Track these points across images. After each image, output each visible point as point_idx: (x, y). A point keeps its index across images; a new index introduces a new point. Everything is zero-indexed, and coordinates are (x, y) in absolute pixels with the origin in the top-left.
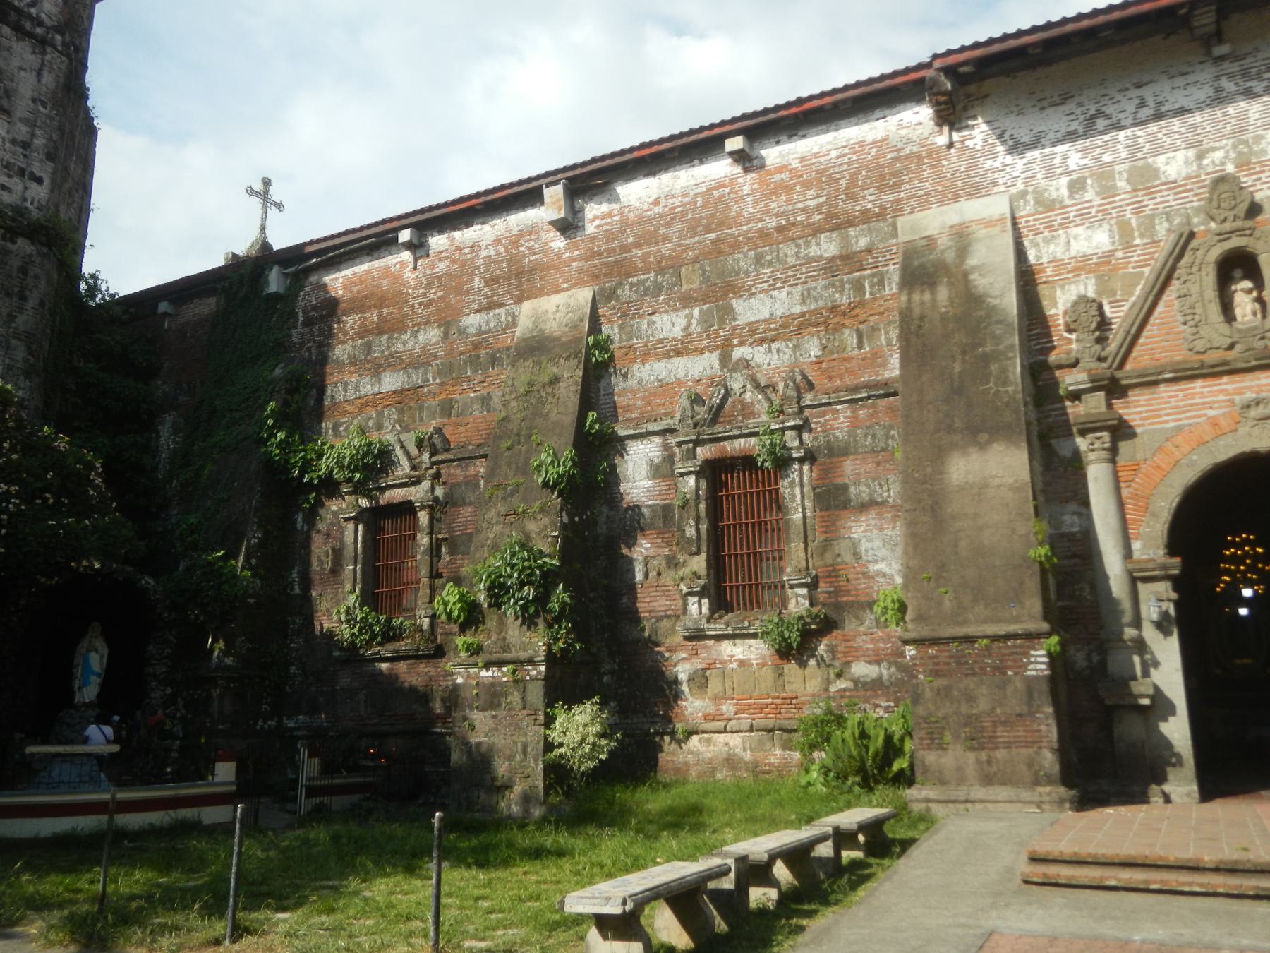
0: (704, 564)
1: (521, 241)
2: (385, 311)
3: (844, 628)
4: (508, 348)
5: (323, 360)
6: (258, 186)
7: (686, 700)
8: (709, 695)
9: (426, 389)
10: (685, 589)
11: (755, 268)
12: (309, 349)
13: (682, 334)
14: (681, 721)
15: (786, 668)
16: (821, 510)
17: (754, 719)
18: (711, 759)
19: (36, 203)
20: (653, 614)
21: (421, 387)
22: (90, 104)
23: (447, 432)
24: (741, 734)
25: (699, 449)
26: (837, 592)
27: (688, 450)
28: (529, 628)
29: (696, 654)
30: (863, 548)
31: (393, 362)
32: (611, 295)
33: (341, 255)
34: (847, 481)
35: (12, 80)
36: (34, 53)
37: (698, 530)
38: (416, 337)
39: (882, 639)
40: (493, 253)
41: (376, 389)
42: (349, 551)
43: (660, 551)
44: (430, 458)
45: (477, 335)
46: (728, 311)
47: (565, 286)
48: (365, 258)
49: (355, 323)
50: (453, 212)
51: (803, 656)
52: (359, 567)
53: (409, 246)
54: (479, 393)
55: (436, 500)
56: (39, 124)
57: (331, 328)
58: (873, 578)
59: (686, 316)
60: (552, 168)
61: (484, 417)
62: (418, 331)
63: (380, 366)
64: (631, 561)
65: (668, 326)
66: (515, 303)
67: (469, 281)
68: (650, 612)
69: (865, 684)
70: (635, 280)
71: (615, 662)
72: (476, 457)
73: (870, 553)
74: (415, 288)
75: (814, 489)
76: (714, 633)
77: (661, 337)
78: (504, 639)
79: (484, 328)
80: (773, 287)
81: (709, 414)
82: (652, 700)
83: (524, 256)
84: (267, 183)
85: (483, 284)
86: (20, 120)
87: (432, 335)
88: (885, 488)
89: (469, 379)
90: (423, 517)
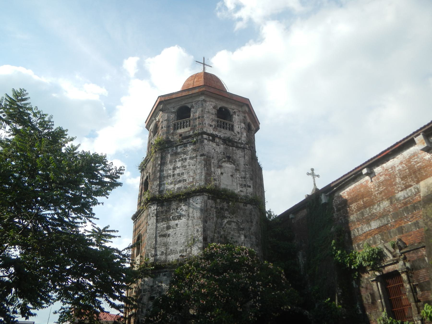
1: (412, 160)
2: (365, 199)
4: (419, 201)
5: (347, 222)
6: (310, 172)
9: (389, 225)
12: (341, 219)
19: (250, 193)
21: (387, 224)
22: (258, 161)
23: (404, 240)
31: (373, 217)
33: (344, 184)
35: (238, 161)
36: (242, 152)
38: (379, 206)
40: (401, 168)
41: (370, 229)
42: (377, 294)
44: (400, 251)
45: (403, 200)
48: (352, 183)
49: (355, 206)
50: (380, 158)
52: (383, 300)
53: (367, 174)
54: (412, 222)
55: (407, 268)
56: (247, 171)
57: (347, 210)
60: (415, 130)
61: (418, 231)
62: (380, 204)
63: (369, 219)
67: (394, 181)
74: (374, 188)
79: (406, 196)
83: (414, 165)
84: (312, 170)
85: (400, 180)
86: (242, 171)
87: (386, 204)
89: (406, 217)
90: (404, 276)
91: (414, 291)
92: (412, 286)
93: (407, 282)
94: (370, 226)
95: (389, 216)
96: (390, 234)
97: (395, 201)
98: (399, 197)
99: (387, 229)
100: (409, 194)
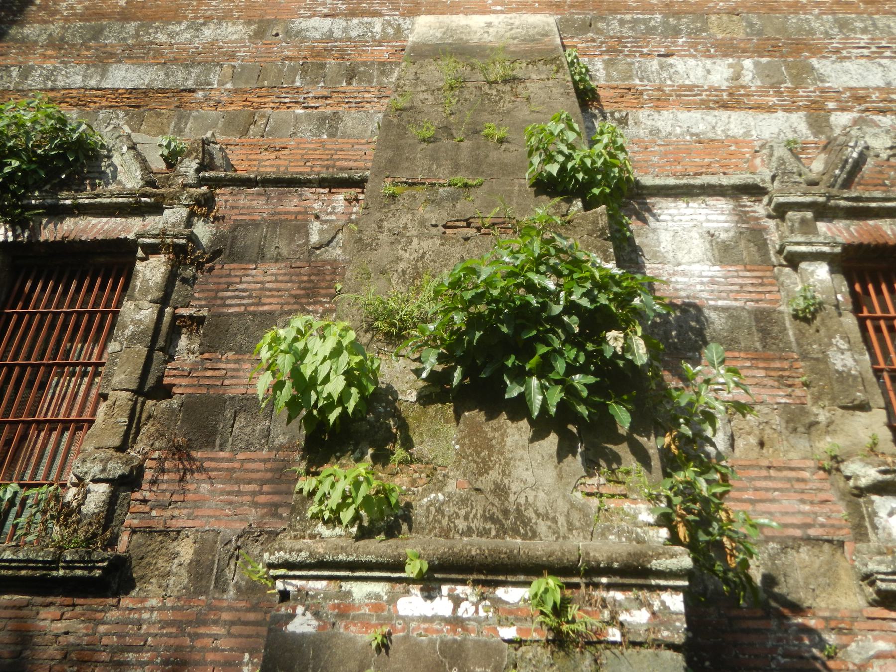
9: (200, 94)
11: (841, 31)
13: (727, 84)
25: (822, 226)
27: (803, 221)
28: (591, 466)
32: (587, 26)
41: (93, 83)
44: (198, 171)
46: (802, 73)
47: (499, 8)
54: (315, 111)
59: (730, 66)
61: (322, 143)
62: (204, 24)
63: (111, 55)
65: (700, 72)
66: (402, 15)
70: (628, 17)
72: (308, 183)
77: (687, 82)
78: (501, 491)
79: (337, 34)
80: (880, 55)
81: (842, 171)
91: (161, 343)
92: (167, 318)
93: (157, 294)
94: (103, 76)
95: (218, 69)
96: (177, 124)
97: (277, 35)
98: (307, 30)
99: (178, 107)
100: (354, 34)
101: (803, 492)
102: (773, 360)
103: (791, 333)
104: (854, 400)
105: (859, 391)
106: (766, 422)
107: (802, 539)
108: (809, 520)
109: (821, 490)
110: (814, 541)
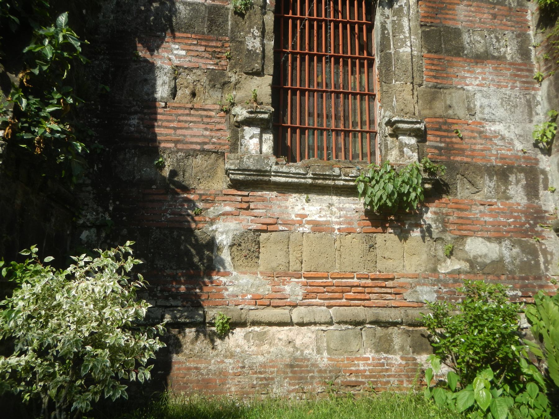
0: (269, 90)
3: (456, 195)
7: (226, 274)
8: (261, 268)
10: (241, 113)
14: (216, 306)
15: (380, 238)
16: (429, 52)
17: (329, 307)
18: (263, 365)
20: (180, 146)
24: (313, 328)
26: (449, 149)
29: (248, 208)
30: (478, 104)
34: (460, 27)
37: (263, 45)
39: (502, 212)
43: (201, 62)
51: (404, 225)
58: (491, 140)
64: (151, 68)
68: (176, 142)
69: (484, 266)
71: (106, 209)
73: (487, 110)
75: (421, 26)
76: (283, 180)
82: (168, 271)
88: (503, 42)
101: (208, 124)
102: (212, 40)
103: (230, 23)
104: (253, 69)
105: (258, 63)
106: (199, 81)
107: (199, 151)
108: (207, 140)
109: (219, 123)
110: (204, 152)
